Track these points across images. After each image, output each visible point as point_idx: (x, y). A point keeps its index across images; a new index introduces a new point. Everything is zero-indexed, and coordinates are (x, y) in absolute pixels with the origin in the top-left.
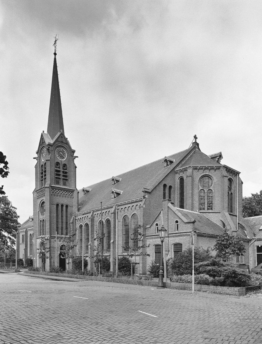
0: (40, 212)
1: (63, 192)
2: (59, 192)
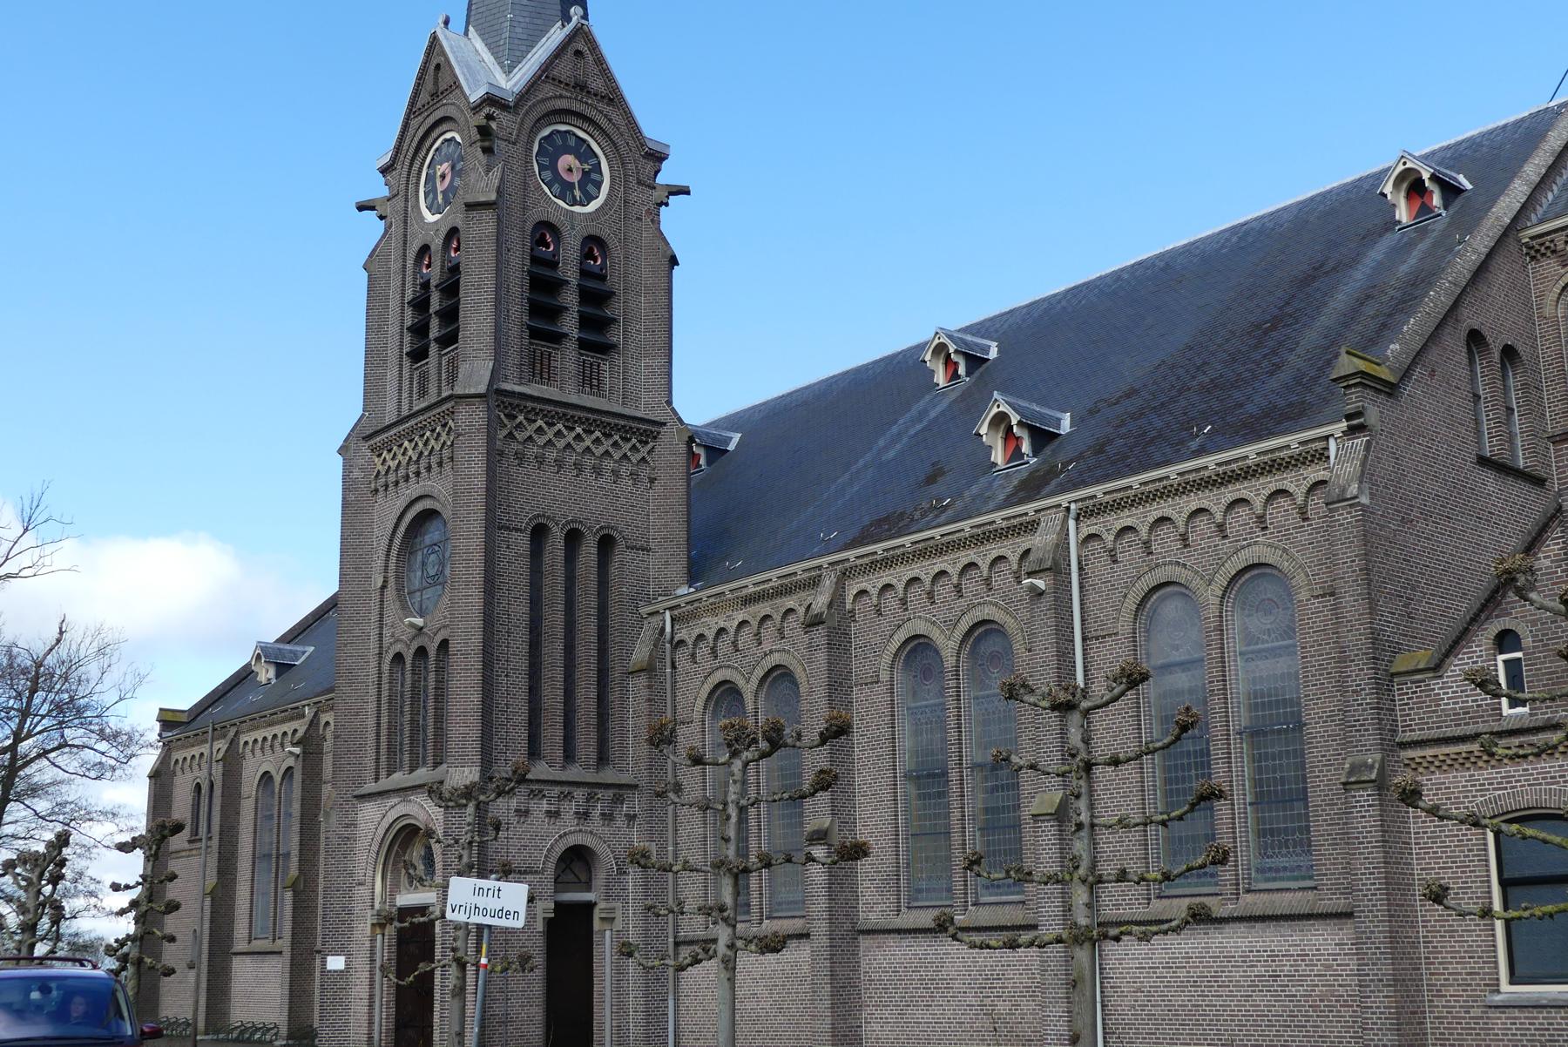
0: (390, 592)
1: (578, 438)
2: (550, 434)
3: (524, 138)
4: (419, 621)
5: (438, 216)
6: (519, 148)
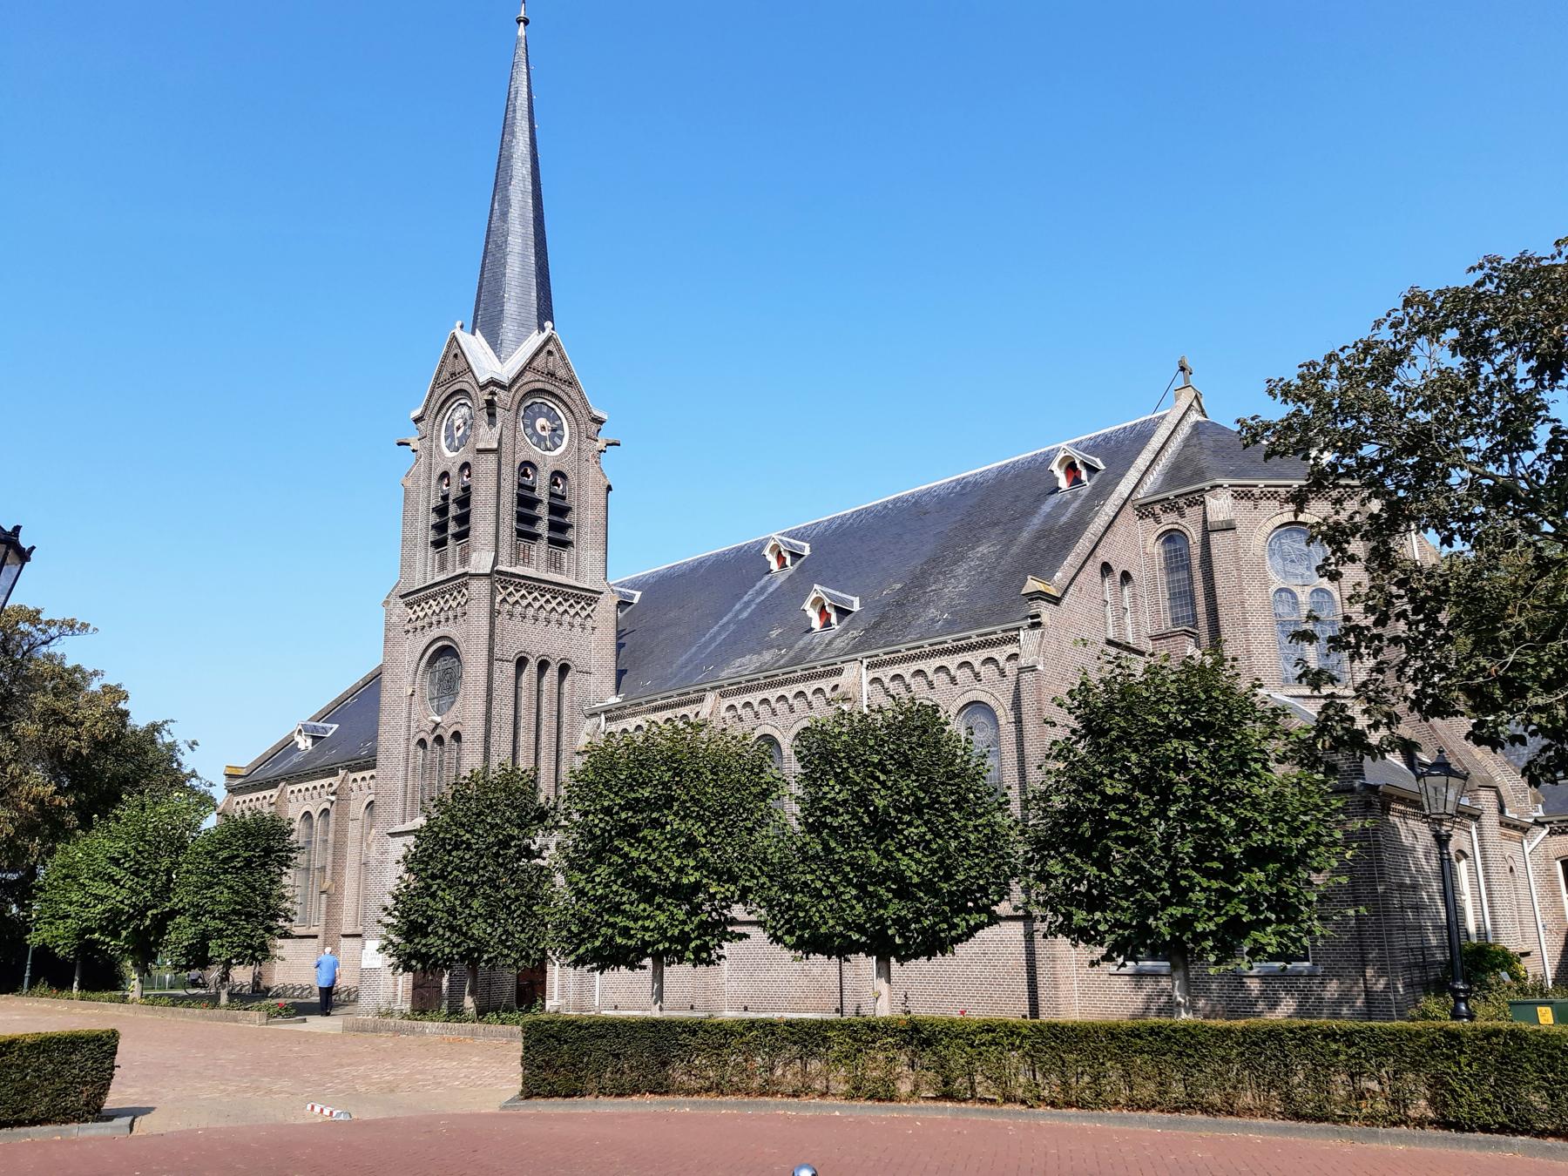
1: (548, 601)
2: (530, 598)
3: (514, 407)
4: (438, 719)
5: (454, 454)
6: (512, 413)
